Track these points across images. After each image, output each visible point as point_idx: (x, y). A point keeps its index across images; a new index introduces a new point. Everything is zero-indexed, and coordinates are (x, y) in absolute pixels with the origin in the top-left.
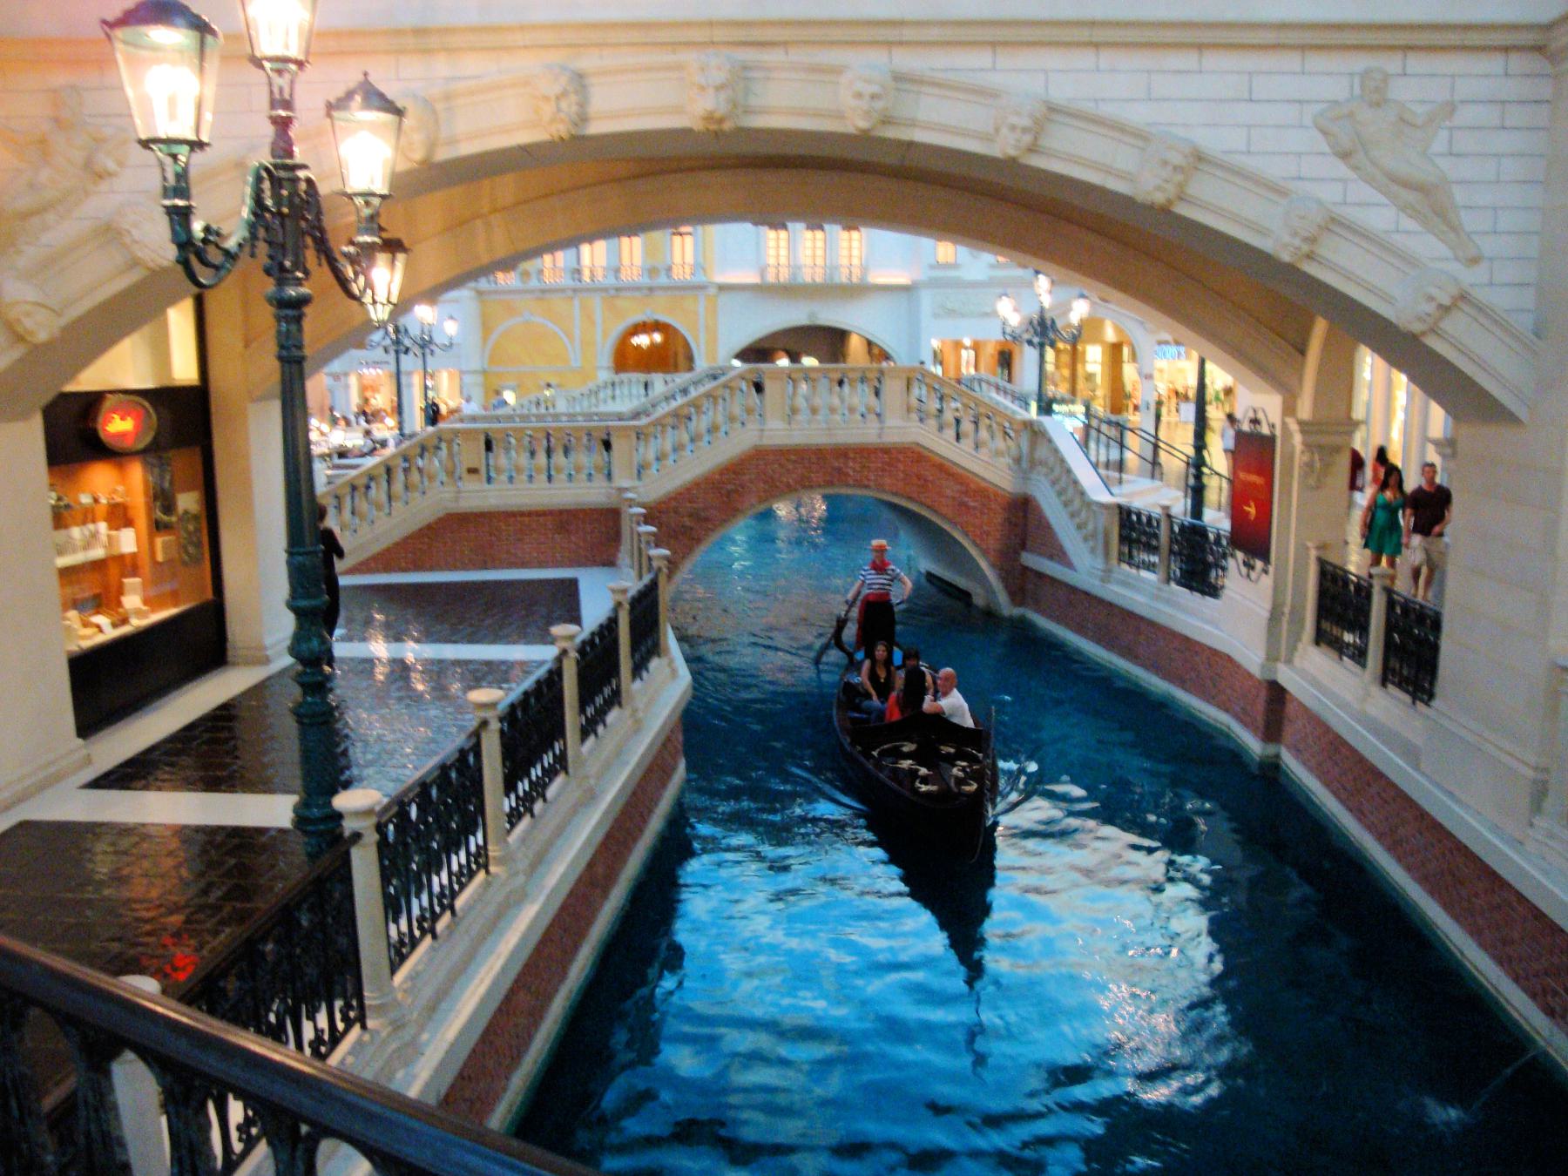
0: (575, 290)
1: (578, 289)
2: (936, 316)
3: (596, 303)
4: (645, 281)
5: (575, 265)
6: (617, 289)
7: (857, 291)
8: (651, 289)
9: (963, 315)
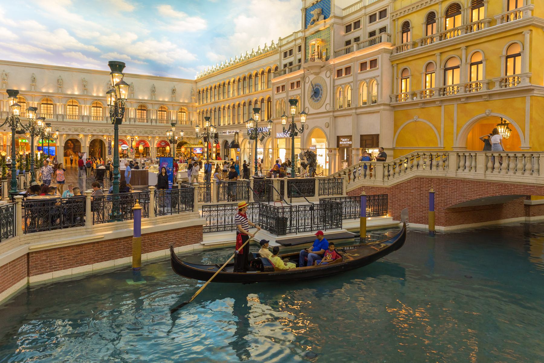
0: (442, 101)
5: (442, 86)
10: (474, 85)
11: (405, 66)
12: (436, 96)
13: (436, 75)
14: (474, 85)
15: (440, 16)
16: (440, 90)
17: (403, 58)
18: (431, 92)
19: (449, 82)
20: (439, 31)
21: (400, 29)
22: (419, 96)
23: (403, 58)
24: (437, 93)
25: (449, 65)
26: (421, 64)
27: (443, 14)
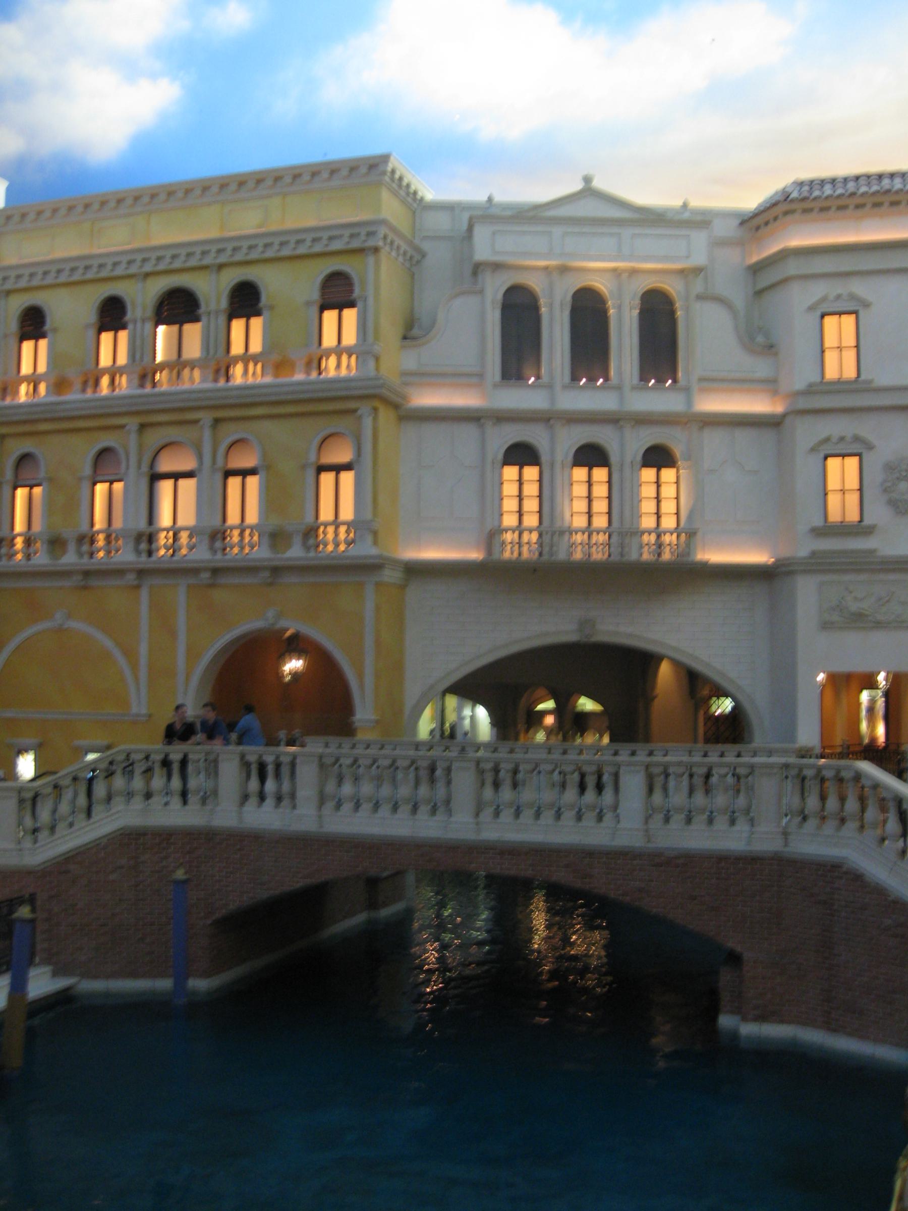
0: (142, 573)
1: (147, 567)
2: (826, 626)
3: (179, 595)
4: (261, 553)
6: (216, 571)
7: (678, 576)
8: (276, 571)
9: (879, 625)
10: (101, 540)
11: (26, 446)
12: (125, 555)
13: (125, 487)
14: (101, 540)
15: (139, 313)
16: (139, 537)
17: (25, 422)
18: (28, 542)
19: (165, 519)
20: (138, 356)
21: (13, 326)
22: (72, 547)
23: (25, 422)
24: (131, 545)
25: (166, 465)
26: (82, 451)
27: (150, 312)
